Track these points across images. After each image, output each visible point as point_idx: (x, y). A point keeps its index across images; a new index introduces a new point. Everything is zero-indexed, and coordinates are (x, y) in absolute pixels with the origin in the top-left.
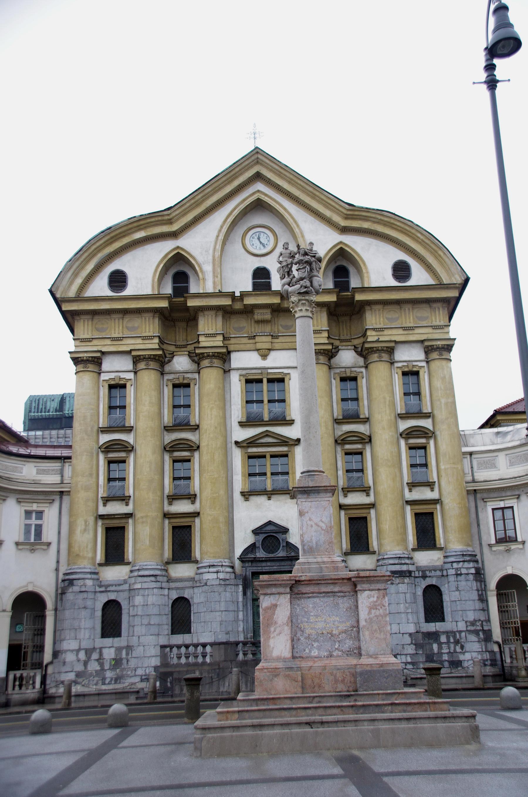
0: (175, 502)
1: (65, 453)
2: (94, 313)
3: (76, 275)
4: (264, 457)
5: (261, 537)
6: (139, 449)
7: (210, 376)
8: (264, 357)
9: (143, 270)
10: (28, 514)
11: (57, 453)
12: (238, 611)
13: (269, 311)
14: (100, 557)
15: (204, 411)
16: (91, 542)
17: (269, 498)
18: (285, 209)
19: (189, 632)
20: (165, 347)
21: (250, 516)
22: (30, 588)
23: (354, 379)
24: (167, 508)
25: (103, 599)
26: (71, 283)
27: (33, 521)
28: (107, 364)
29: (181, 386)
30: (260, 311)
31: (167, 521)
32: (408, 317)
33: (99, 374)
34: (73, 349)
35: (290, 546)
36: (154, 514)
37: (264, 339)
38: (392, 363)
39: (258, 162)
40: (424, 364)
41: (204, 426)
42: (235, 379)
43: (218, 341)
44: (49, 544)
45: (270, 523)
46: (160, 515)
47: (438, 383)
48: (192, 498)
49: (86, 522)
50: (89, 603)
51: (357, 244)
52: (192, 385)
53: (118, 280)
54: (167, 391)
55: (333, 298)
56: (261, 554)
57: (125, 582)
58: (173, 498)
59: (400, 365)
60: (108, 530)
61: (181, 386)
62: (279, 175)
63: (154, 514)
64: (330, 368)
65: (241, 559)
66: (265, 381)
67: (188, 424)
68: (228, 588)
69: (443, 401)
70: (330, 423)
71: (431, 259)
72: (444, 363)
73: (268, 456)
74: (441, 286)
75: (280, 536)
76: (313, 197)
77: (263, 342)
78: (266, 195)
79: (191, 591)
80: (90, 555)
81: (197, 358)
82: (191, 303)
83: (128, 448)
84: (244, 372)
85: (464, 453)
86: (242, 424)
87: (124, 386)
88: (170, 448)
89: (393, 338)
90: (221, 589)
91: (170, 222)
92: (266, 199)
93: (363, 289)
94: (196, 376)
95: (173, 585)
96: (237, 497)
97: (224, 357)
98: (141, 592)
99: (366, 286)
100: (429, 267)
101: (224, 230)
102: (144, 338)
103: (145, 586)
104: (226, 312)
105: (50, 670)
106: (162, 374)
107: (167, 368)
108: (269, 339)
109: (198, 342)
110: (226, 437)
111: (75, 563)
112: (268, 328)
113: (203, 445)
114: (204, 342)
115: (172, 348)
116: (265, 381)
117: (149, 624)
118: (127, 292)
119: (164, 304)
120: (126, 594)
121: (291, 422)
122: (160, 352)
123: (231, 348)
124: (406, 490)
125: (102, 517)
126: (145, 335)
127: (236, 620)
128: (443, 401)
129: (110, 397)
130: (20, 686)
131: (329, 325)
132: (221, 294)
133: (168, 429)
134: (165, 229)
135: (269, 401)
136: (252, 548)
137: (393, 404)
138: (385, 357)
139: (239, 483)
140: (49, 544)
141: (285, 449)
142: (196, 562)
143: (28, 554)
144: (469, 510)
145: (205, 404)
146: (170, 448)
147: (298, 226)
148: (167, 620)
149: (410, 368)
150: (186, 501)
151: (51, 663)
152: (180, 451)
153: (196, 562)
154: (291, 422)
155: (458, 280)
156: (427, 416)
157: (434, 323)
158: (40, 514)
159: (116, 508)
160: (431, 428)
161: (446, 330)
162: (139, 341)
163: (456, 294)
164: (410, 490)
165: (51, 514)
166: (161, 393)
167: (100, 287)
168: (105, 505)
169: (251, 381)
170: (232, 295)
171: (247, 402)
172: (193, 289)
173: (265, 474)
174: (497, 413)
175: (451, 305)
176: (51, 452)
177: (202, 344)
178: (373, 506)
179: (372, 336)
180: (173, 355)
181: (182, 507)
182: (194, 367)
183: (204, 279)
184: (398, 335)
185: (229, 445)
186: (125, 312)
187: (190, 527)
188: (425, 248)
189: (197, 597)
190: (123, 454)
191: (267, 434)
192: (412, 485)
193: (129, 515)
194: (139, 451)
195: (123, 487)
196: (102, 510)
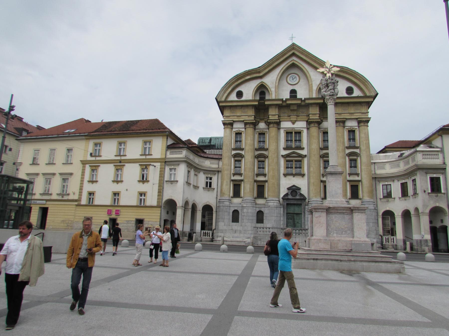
0: (259, 177)
1: (220, 157)
2: (231, 107)
3: (225, 92)
4: (292, 161)
6: (246, 157)
7: (273, 130)
8: (293, 124)
9: (249, 91)
10: (207, 178)
11: (217, 157)
12: (281, 217)
13: (296, 106)
14: (231, 194)
15: (269, 143)
16: (229, 190)
17: (294, 177)
18: (304, 67)
19: (263, 223)
20: (256, 119)
21: (286, 183)
22: (208, 204)
24: (256, 178)
25: (232, 209)
27: (209, 181)
28: (235, 125)
29: (262, 134)
31: (255, 183)
32: (352, 110)
33: (232, 129)
34: (223, 119)
35: (301, 195)
36: (251, 180)
37: (294, 117)
38: (344, 127)
39: (293, 49)
40: (357, 127)
43: (276, 118)
44: (214, 189)
45: (294, 186)
46: (253, 181)
47: (363, 135)
48: (265, 175)
49: (227, 182)
52: (266, 134)
53: (240, 94)
54: (257, 136)
57: (240, 204)
58: (258, 175)
59: (347, 128)
60: (235, 185)
61: (262, 134)
62: (302, 53)
63: (251, 180)
64: (319, 128)
65: (282, 198)
66: (293, 133)
67: (264, 148)
68: (278, 208)
69: (364, 142)
70: (318, 149)
71: (362, 86)
72: (366, 127)
73: (294, 161)
74: (366, 97)
75: (298, 191)
76: (315, 62)
77: (293, 118)
78: (296, 61)
79: (264, 208)
80: (228, 194)
81: (268, 124)
82: (266, 103)
83: (241, 156)
84: (286, 129)
85: (372, 163)
86: (284, 149)
87: (241, 134)
88: (257, 157)
89: (345, 117)
90: (275, 208)
91: (259, 72)
92: (296, 63)
94: (267, 130)
95: (257, 206)
96: (282, 175)
98: (246, 208)
100: (361, 89)
101: (280, 75)
102: (249, 116)
103: (248, 206)
104: (280, 107)
105: (215, 231)
106: (255, 129)
107: (257, 127)
108: (296, 117)
109: (269, 117)
110: (278, 153)
111: (223, 196)
112: (295, 113)
113: (270, 156)
114: (271, 117)
115: (259, 120)
116: (293, 133)
117: (249, 219)
119: (256, 103)
120: (241, 208)
121: (303, 149)
122: (255, 121)
123: (281, 120)
124: (348, 176)
125: (233, 180)
126: (249, 115)
127: (280, 220)
128: (364, 142)
129: (236, 137)
130: (205, 236)
131: (320, 112)
133: (256, 150)
135: (295, 140)
136: (287, 195)
138: (342, 124)
139: (282, 170)
140: (214, 189)
141: (300, 159)
143: (207, 192)
144: (372, 185)
146: (257, 157)
147: (308, 73)
148: (255, 218)
149: (352, 129)
150: (262, 176)
151: (215, 229)
152: (261, 158)
153: (266, 198)
154: (303, 149)
155: (373, 94)
156: (357, 148)
157: (362, 112)
158: (211, 179)
160: (359, 152)
161: (367, 114)
162: (247, 117)
163: (372, 100)
164: (349, 176)
165: (215, 178)
166: (254, 136)
168: (233, 176)
169: (288, 133)
170: (282, 100)
171: (287, 140)
172: (267, 98)
173: (292, 168)
174: (386, 147)
175: (369, 104)
176: (214, 157)
177: (270, 119)
180: (259, 122)
181: (261, 178)
182: (267, 127)
183: (272, 94)
185: (279, 156)
186: (242, 106)
187: (264, 186)
188: (360, 81)
190: (240, 158)
192: (350, 174)
194: (246, 157)
195: (240, 170)
196: (233, 178)
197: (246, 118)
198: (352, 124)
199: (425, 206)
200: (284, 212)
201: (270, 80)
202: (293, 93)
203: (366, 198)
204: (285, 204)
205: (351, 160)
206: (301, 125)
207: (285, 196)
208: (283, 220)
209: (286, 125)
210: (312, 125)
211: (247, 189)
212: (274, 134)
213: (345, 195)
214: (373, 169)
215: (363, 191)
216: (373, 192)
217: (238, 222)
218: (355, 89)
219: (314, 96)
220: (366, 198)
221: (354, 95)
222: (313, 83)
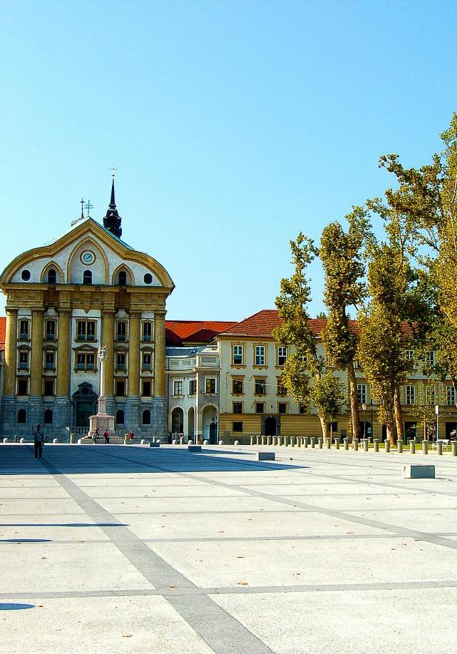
3: (9, 273)
5: (82, 388)
8: (87, 313)
9: (37, 271)
15: (60, 334)
26: (7, 276)
30: (87, 289)
42: (74, 321)
45: (85, 383)
47: (158, 329)
48: (54, 370)
50: (13, 410)
51: (130, 264)
53: (26, 275)
56: (81, 395)
58: (46, 370)
65: (73, 396)
67: (53, 339)
74: (163, 288)
75: (89, 388)
77: (87, 304)
93: (130, 287)
95: (46, 405)
96: (72, 371)
97: (69, 314)
99: (133, 285)
100: (159, 278)
118: (30, 281)
120: (27, 408)
125: (18, 376)
142: (55, 396)
145: (61, 332)
153: (55, 396)
155: (170, 286)
156: (152, 342)
159: (23, 373)
175: (167, 295)
178: (127, 377)
179: (133, 307)
181: (50, 374)
189: (55, 410)
193: (28, 376)
196: (18, 373)
197: (34, 304)
198: (149, 316)
200: (74, 411)
201: (62, 260)
203: (157, 395)
204: (76, 403)
206: (95, 314)
207: (75, 394)
208: (74, 420)
209: (79, 313)
210: (106, 315)
211: (34, 387)
212: (64, 324)
214: (167, 365)
215: (156, 389)
216: (165, 389)
217: (24, 422)
220: (157, 395)
222: (110, 266)
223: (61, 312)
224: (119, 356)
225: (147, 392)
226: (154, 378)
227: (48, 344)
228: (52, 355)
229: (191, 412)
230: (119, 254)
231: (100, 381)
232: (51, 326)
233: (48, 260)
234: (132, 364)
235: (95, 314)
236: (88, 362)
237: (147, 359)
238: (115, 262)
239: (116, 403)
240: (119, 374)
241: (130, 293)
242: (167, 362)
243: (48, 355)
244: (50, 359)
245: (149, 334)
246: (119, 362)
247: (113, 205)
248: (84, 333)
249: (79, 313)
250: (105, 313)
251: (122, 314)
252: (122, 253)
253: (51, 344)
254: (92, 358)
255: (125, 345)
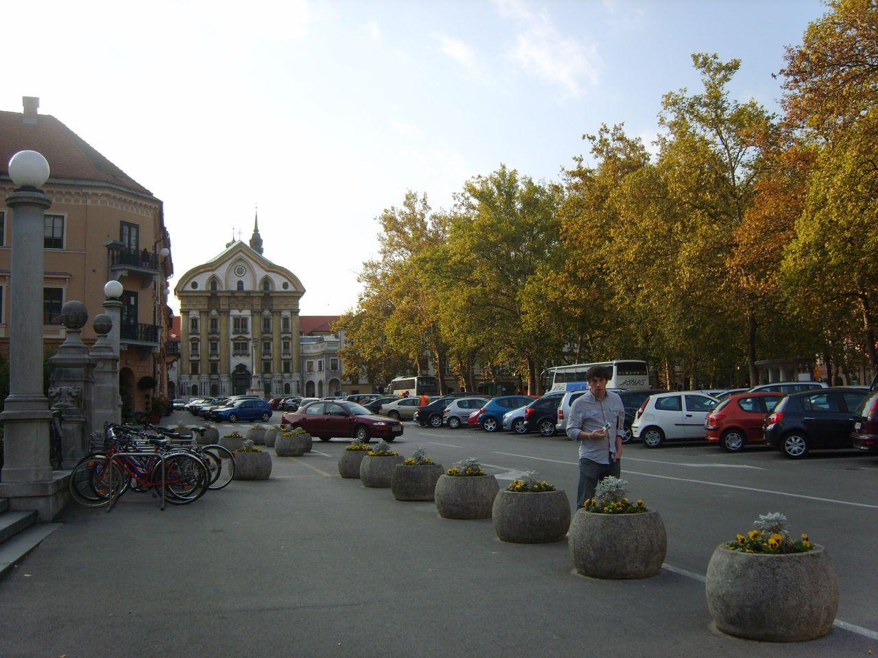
8: (240, 312)
9: (203, 283)
15: (221, 328)
21: (235, 361)
23: (268, 320)
28: (190, 313)
30: (240, 297)
41: (221, 334)
42: (231, 318)
47: (294, 324)
48: (217, 355)
51: (272, 275)
53: (195, 285)
54: (210, 321)
55: (263, 295)
58: (211, 356)
60: (192, 365)
64: (261, 316)
65: (233, 374)
81: (219, 312)
83: (198, 340)
96: (231, 356)
97: (227, 313)
99: (274, 290)
100: (294, 285)
113: (221, 340)
114: (222, 307)
118: (197, 289)
121: (248, 333)
132: (229, 291)
133: (209, 333)
134: (210, 268)
135: (242, 326)
136: (234, 371)
137: (280, 329)
138: (278, 314)
156: (290, 333)
159: (195, 358)
167: (189, 288)
169: (237, 320)
175: (299, 297)
178: (272, 359)
179: (275, 308)
180: (211, 309)
181: (215, 358)
184: (282, 307)
191: (241, 337)
192: (284, 354)
198: (286, 314)
199: (327, 378)
202: (240, 284)
205: (284, 343)
206: (246, 313)
209: (235, 312)
211: (204, 367)
213: (280, 371)
214: (301, 350)
218: (289, 283)
219: (257, 289)
221: (288, 290)
223: (221, 312)
224: (265, 343)
225: (287, 370)
226: (291, 359)
227: (212, 336)
228: (216, 344)
229: (321, 383)
230: (263, 268)
231: (250, 362)
232: (214, 323)
233: (210, 274)
234: (276, 350)
235: (246, 313)
236: (242, 349)
237: (286, 346)
238: (261, 274)
239: (265, 379)
240: (266, 357)
241: (272, 297)
242: (301, 347)
243: (212, 344)
244: (214, 347)
245: (288, 327)
246: (265, 348)
247: (256, 230)
248: (239, 327)
249: (235, 312)
250: (255, 312)
251: (267, 312)
252: (265, 267)
253: (216, 336)
254: (245, 346)
255: (270, 335)
